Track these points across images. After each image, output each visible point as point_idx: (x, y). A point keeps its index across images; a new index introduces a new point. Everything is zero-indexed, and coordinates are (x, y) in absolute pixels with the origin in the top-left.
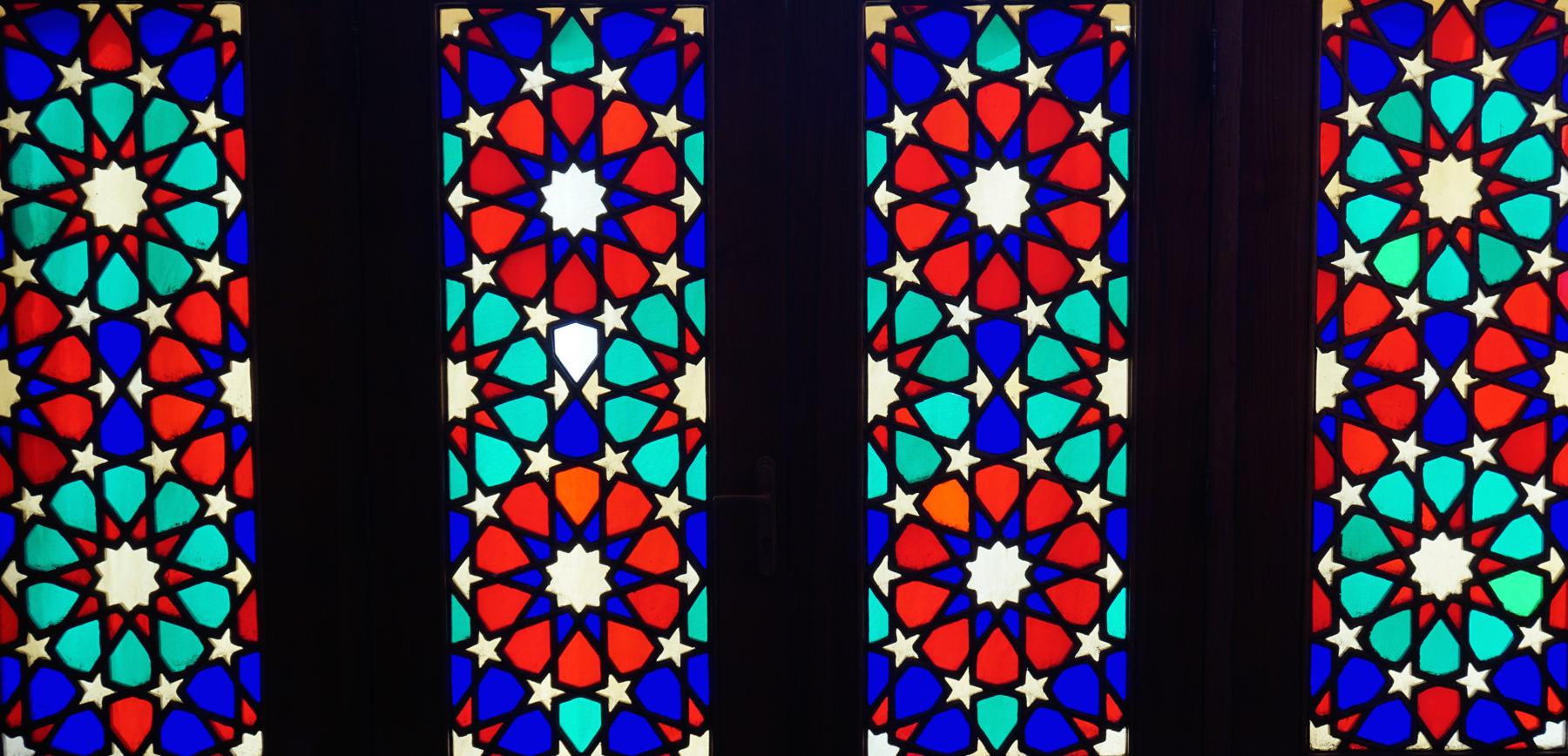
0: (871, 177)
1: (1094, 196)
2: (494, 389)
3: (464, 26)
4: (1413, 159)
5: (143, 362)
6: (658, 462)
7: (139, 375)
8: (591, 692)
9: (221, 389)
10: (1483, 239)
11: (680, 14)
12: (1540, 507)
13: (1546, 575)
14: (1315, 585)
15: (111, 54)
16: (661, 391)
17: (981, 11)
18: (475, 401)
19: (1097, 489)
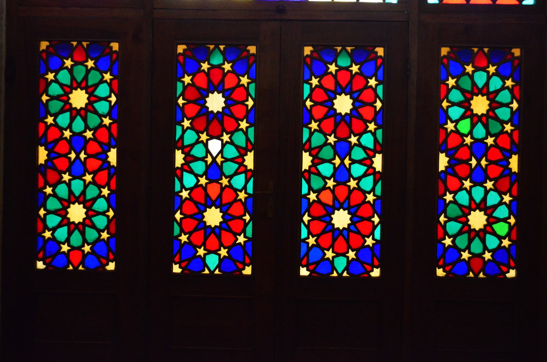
0: (305, 97)
1: (372, 104)
2: (189, 159)
3: (184, 50)
4: (469, 96)
5: (84, 148)
6: (239, 181)
7: (83, 152)
8: (215, 252)
9: (108, 157)
10: (490, 120)
11: (249, 48)
12: (508, 202)
13: (509, 223)
14: (439, 225)
15: (78, 56)
16: (240, 160)
17: (339, 49)
18: (184, 162)
19: (372, 193)
